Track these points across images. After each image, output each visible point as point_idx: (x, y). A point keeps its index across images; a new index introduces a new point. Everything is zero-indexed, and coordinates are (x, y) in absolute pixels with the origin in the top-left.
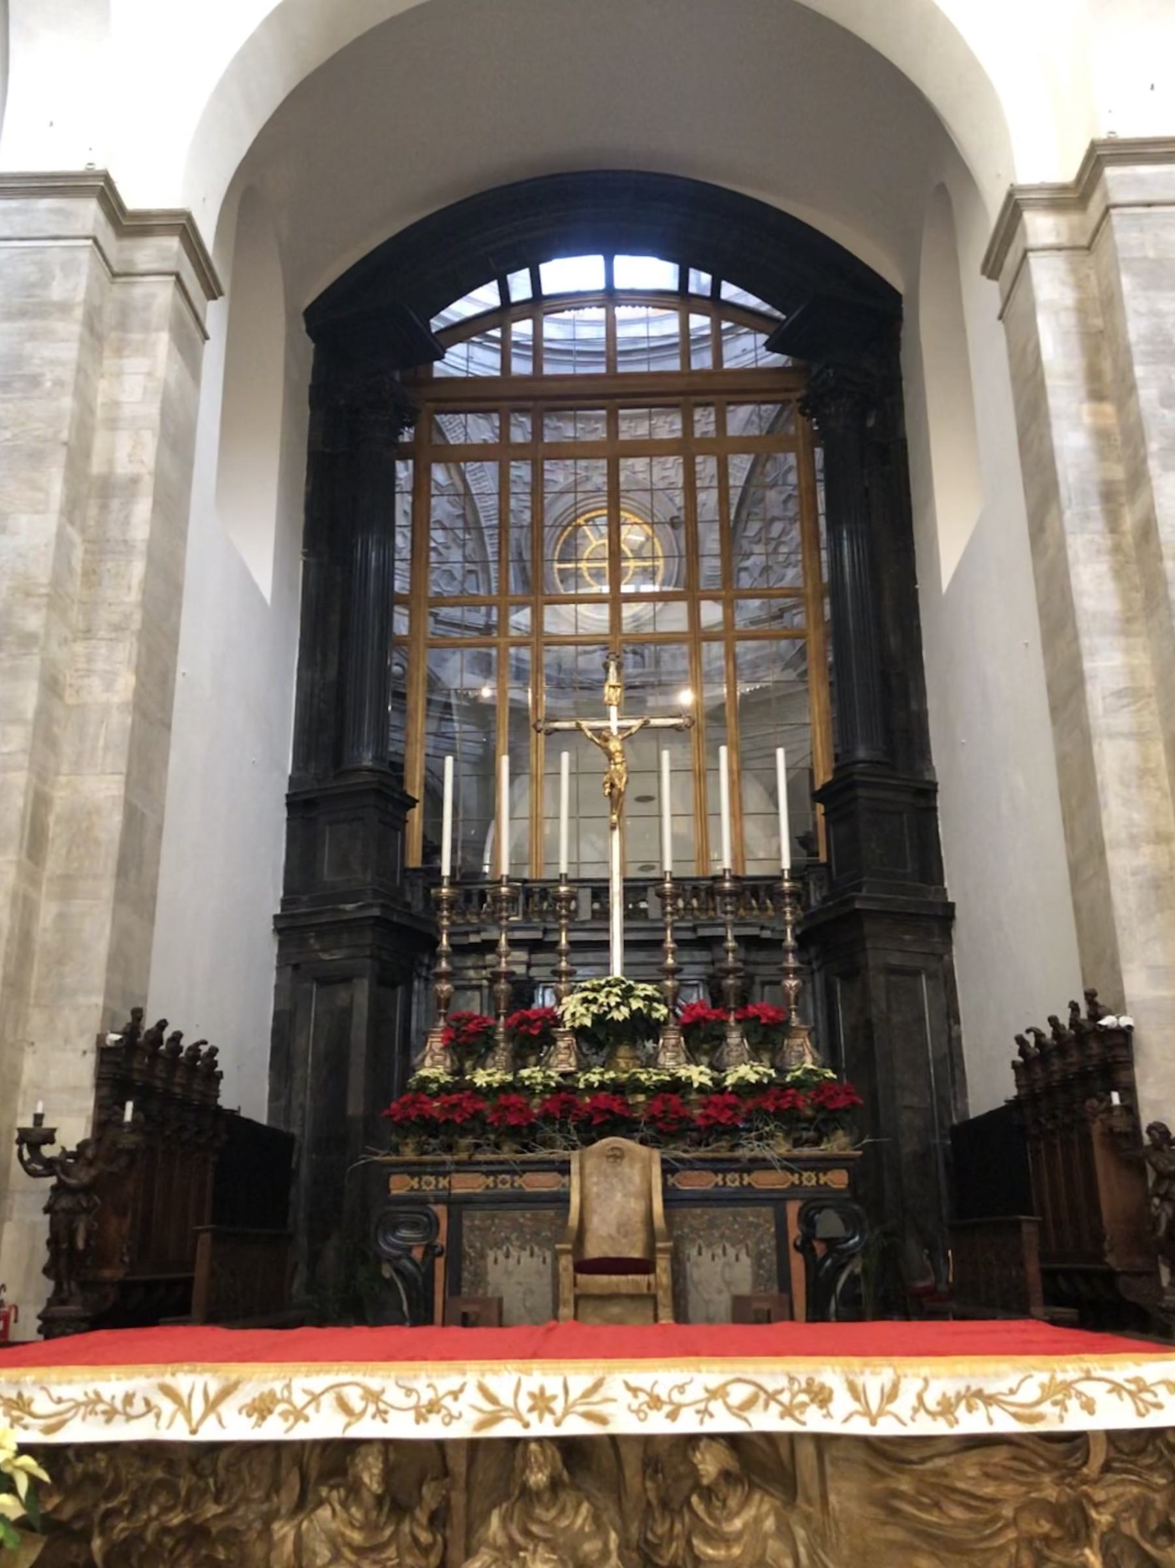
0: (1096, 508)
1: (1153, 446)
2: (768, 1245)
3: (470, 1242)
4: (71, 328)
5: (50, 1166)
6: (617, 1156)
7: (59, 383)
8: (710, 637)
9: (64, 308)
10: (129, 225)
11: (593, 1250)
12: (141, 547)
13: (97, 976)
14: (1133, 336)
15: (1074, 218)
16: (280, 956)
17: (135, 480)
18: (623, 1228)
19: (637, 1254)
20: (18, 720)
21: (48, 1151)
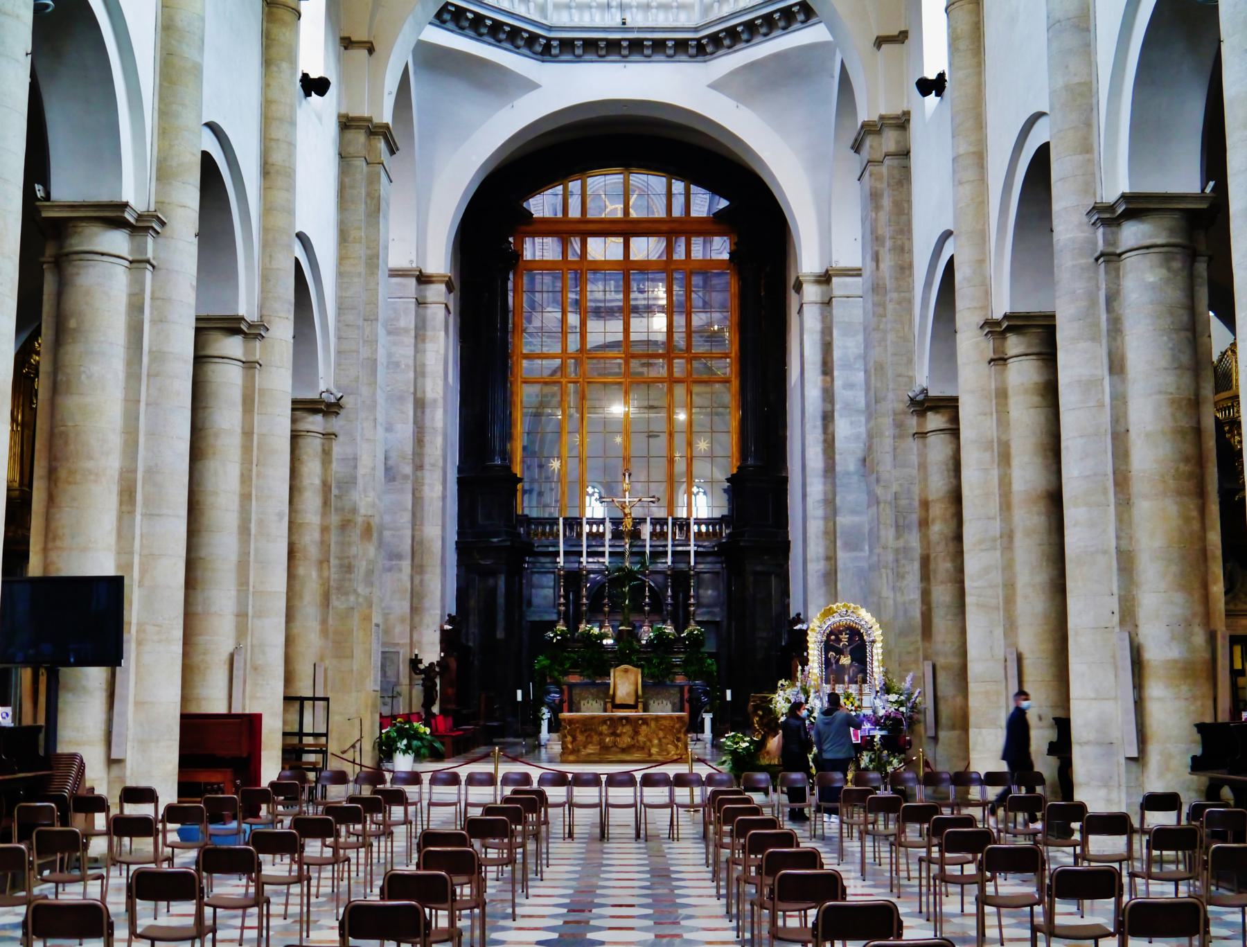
0: (819, 423)
1: (837, 407)
2: (677, 700)
3: (576, 698)
4: (409, 340)
5: (422, 672)
6: (626, 671)
7: (407, 365)
8: (679, 381)
9: (406, 330)
10: (423, 279)
11: (618, 701)
13: (438, 604)
14: (835, 358)
15: (824, 287)
16: (458, 561)
17: (435, 401)
18: (628, 694)
19: (632, 703)
20: (406, 510)
21: (422, 667)
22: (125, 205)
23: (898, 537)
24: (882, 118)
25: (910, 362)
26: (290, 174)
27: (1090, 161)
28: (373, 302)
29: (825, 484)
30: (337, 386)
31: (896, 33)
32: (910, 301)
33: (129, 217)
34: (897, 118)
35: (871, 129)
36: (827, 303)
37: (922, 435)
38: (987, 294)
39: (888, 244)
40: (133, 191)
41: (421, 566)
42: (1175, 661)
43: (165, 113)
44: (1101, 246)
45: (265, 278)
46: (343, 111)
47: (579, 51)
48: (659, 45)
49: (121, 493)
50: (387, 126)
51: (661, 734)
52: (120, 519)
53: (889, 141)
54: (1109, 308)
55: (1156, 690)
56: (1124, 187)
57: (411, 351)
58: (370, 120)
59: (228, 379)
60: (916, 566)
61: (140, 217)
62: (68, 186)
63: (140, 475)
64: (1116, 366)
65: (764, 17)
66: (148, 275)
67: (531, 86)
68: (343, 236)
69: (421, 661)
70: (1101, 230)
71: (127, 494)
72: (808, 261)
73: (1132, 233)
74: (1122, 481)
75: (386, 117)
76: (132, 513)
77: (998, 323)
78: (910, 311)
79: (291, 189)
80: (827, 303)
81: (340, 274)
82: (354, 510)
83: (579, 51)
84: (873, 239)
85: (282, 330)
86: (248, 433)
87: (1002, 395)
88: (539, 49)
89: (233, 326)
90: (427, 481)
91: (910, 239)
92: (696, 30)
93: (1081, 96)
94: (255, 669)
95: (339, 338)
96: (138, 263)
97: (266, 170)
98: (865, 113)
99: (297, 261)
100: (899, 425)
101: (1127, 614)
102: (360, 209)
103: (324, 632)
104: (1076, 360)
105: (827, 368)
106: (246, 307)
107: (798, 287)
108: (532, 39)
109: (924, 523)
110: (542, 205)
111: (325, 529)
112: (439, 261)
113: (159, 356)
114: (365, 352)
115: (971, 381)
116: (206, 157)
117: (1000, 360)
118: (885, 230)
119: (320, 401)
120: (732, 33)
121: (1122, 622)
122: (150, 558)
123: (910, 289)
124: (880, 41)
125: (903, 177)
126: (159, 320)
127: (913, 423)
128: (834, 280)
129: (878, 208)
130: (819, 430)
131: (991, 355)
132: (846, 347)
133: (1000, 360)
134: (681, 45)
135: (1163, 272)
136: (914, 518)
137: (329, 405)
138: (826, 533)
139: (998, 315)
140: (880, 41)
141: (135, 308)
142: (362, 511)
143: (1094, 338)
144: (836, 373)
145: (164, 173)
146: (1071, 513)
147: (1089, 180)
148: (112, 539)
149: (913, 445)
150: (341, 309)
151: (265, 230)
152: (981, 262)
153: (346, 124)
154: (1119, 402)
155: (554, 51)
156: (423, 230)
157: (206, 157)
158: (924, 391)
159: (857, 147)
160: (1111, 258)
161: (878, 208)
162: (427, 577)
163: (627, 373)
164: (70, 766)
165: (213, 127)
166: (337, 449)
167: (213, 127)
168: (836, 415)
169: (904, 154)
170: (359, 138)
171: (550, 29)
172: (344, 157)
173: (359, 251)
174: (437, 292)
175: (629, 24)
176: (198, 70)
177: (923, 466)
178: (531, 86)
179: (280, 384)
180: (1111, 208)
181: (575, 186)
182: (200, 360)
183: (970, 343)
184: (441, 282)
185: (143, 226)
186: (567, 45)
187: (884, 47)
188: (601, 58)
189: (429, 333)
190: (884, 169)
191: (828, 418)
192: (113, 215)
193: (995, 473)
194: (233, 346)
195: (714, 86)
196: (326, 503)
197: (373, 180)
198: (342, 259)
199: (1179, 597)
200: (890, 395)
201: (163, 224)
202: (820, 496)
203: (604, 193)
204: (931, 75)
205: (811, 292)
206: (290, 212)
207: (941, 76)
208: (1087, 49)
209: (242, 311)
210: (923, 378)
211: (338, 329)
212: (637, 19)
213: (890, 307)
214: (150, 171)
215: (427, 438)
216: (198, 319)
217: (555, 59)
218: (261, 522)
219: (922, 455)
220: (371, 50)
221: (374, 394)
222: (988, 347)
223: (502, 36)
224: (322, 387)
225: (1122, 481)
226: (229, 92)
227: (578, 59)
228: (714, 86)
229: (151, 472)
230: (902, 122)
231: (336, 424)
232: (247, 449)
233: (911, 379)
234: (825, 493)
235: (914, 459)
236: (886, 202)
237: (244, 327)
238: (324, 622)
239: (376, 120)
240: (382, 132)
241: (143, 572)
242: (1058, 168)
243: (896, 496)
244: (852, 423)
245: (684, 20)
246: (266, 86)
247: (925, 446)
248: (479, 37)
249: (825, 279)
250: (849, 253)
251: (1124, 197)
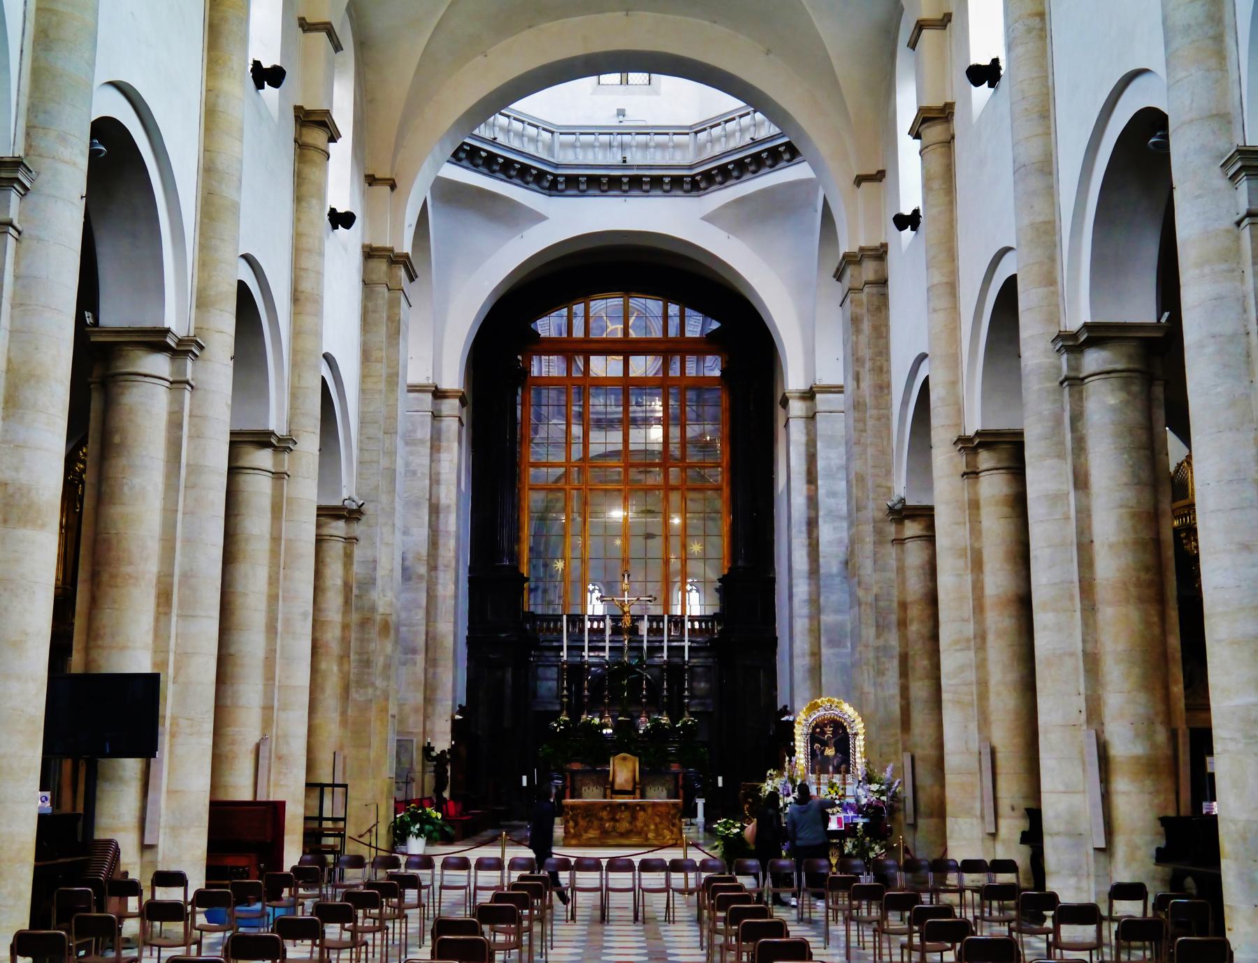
0: (804, 528)
1: (821, 513)
4: (426, 450)
5: (434, 759)
6: (624, 759)
7: (423, 474)
9: (422, 442)
10: (439, 394)
11: (617, 787)
12: (453, 534)
13: (449, 696)
15: (809, 403)
17: (449, 506)
18: (626, 781)
19: (629, 788)
20: (420, 607)
21: (434, 754)
22: (168, 331)
23: (878, 636)
24: (862, 249)
25: (888, 473)
26: (318, 300)
27: (1055, 293)
28: (392, 417)
29: (810, 585)
30: (358, 494)
31: (874, 172)
32: (888, 418)
33: (171, 342)
34: (875, 249)
35: (851, 260)
36: (811, 418)
37: (900, 541)
38: (959, 412)
39: (868, 365)
40: (175, 317)
41: (435, 660)
42: (1137, 759)
43: (205, 245)
44: (1065, 371)
45: (294, 396)
46: (367, 242)
47: (583, 187)
48: (656, 182)
49: (158, 596)
50: (407, 255)
51: (657, 820)
52: (157, 620)
53: (869, 270)
54: (1074, 429)
55: (1122, 785)
56: (1086, 317)
57: (427, 461)
58: (391, 250)
59: (259, 488)
60: (896, 663)
61: (181, 342)
62: (116, 313)
63: (176, 580)
64: (1081, 481)
65: (753, 156)
66: (187, 394)
67: (540, 218)
68: (366, 355)
69: (433, 749)
70: (1065, 356)
71: (164, 597)
72: (794, 379)
73: (1094, 360)
74: (1087, 587)
75: (406, 247)
76: (168, 614)
77: (970, 439)
78: (888, 427)
79: (319, 314)
80: (811, 418)
81: (363, 391)
82: (373, 609)
83: (583, 187)
84: (854, 361)
85: (309, 443)
86: (276, 539)
87: (974, 505)
88: (547, 184)
89: (263, 440)
90: (441, 581)
91: (888, 360)
92: (690, 167)
93: (1046, 232)
94: (279, 758)
95: (361, 450)
96: (178, 384)
97: (296, 297)
98: (846, 245)
99: (323, 378)
100: (879, 532)
101: (1094, 712)
102: (382, 332)
103: (344, 722)
104: (1043, 477)
105: (811, 478)
106: (276, 423)
107: (785, 402)
108: (541, 175)
109: (903, 624)
110: (548, 326)
111: (345, 627)
112: (453, 378)
113: (195, 469)
114: (384, 462)
115: (945, 492)
116: (242, 286)
117: (972, 474)
118: (866, 352)
119: (343, 508)
121: (1089, 720)
122: (184, 656)
123: (888, 407)
124: (860, 180)
125: (881, 304)
126: (197, 436)
127: (891, 529)
128: (818, 396)
129: (858, 331)
130: (804, 535)
131: (964, 469)
132: (829, 457)
133: (972, 474)
134: (677, 182)
135: (1122, 395)
136: (894, 618)
137: (351, 511)
138: (811, 630)
139: (970, 432)
140: (860, 180)
141: (175, 424)
142: (381, 610)
143: (1060, 456)
144: (820, 482)
145: (203, 302)
146: (1041, 618)
147: (1053, 310)
148: (149, 638)
149: (892, 551)
150: (363, 423)
151: (295, 352)
152: (954, 383)
153: (370, 253)
154: (1084, 515)
155: (560, 187)
156: (439, 348)
157: (242, 286)
158: (902, 500)
159: (839, 276)
160: (1074, 382)
161: (858, 331)
162: (440, 670)
163: (626, 481)
164: (106, 851)
165: (248, 258)
166: (358, 552)
167: (248, 258)
168: (820, 520)
169: (882, 282)
170: (381, 266)
171: (557, 166)
172: (367, 283)
173: (381, 369)
174: (451, 407)
175: (630, 162)
176: (235, 207)
177: (901, 570)
178: (540, 218)
179: (307, 493)
180: (1074, 336)
181: (579, 308)
182: (234, 471)
183: (944, 458)
184: (455, 397)
185: (185, 350)
186: (572, 181)
187: (864, 185)
188: (604, 193)
189: (444, 444)
190: (864, 297)
191: (812, 524)
192: (156, 340)
193: (969, 578)
194: (263, 458)
195: (709, 218)
196: (347, 601)
197: (393, 305)
198: (364, 377)
199: (1142, 697)
200: (871, 505)
201: (201, 348)
202: (805, 597)
203: (606, 314)
204: (907, 211)
205: (797, 408)
206: (318, 335)
207: (916, 212)
208: (1051, 192)
209: (272, 426)
210: (900, 488)
211: (360, 442)
212: (636, 158)
213: (870, 423)
214: (191, 300)
215: (441, 542)
216: (232, 434)
217: (561, 194)
218: (287, 621)
219: (900, 560)
220: (393, 187)
221: (393, 501)
222: (961, 462)
223: (513, 173)
224: (345, 495)
225: (1087, 587)
226: (262, 225)
227: (583, 194)
228: (709, 218)
229: (185, 577)
230: (880, 253)
231: (358, 529)
232: (275, 553)
233: (890, 489)
234: (810, 594)
235: (893, 563)
236: (866, 326)
237: (274, 441)
238: (344, 713)
239: (397, 250)
240: (402, 261)
241: (177, 669)
242: (1027, 299)
243: (877, 598)
244: (835, 529)
245: (680, 158)
246: (297, 220)
247: (903, 551)
248: (491, 173)
249: (809, 395)
250: (831, 371)
251: (1086, 326)
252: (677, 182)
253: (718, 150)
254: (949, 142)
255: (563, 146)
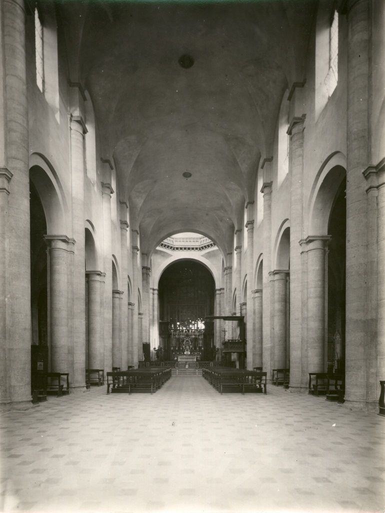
35: (226, 269)
56: (256, 288)
67: (169, 255)
72: (217, 287)
108: (171, 248)
120: (205, 247)
124: (228, 254)
134: (197, 249)
140: (228, 254)
178: (169, 255)
186: (177, 249)
195: (202, 256)
228: (202, 256)
252: (197, 249)
253: (205, 242)
254: (240, 252)
255: (176, 241)
